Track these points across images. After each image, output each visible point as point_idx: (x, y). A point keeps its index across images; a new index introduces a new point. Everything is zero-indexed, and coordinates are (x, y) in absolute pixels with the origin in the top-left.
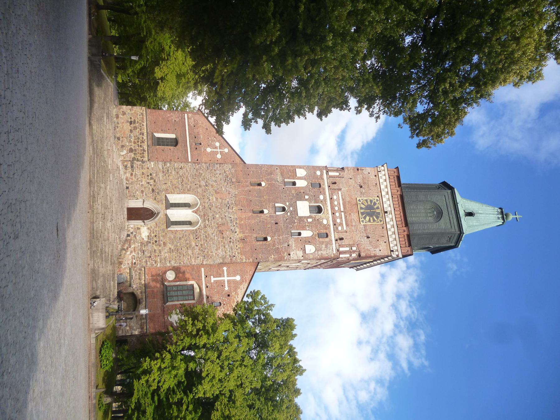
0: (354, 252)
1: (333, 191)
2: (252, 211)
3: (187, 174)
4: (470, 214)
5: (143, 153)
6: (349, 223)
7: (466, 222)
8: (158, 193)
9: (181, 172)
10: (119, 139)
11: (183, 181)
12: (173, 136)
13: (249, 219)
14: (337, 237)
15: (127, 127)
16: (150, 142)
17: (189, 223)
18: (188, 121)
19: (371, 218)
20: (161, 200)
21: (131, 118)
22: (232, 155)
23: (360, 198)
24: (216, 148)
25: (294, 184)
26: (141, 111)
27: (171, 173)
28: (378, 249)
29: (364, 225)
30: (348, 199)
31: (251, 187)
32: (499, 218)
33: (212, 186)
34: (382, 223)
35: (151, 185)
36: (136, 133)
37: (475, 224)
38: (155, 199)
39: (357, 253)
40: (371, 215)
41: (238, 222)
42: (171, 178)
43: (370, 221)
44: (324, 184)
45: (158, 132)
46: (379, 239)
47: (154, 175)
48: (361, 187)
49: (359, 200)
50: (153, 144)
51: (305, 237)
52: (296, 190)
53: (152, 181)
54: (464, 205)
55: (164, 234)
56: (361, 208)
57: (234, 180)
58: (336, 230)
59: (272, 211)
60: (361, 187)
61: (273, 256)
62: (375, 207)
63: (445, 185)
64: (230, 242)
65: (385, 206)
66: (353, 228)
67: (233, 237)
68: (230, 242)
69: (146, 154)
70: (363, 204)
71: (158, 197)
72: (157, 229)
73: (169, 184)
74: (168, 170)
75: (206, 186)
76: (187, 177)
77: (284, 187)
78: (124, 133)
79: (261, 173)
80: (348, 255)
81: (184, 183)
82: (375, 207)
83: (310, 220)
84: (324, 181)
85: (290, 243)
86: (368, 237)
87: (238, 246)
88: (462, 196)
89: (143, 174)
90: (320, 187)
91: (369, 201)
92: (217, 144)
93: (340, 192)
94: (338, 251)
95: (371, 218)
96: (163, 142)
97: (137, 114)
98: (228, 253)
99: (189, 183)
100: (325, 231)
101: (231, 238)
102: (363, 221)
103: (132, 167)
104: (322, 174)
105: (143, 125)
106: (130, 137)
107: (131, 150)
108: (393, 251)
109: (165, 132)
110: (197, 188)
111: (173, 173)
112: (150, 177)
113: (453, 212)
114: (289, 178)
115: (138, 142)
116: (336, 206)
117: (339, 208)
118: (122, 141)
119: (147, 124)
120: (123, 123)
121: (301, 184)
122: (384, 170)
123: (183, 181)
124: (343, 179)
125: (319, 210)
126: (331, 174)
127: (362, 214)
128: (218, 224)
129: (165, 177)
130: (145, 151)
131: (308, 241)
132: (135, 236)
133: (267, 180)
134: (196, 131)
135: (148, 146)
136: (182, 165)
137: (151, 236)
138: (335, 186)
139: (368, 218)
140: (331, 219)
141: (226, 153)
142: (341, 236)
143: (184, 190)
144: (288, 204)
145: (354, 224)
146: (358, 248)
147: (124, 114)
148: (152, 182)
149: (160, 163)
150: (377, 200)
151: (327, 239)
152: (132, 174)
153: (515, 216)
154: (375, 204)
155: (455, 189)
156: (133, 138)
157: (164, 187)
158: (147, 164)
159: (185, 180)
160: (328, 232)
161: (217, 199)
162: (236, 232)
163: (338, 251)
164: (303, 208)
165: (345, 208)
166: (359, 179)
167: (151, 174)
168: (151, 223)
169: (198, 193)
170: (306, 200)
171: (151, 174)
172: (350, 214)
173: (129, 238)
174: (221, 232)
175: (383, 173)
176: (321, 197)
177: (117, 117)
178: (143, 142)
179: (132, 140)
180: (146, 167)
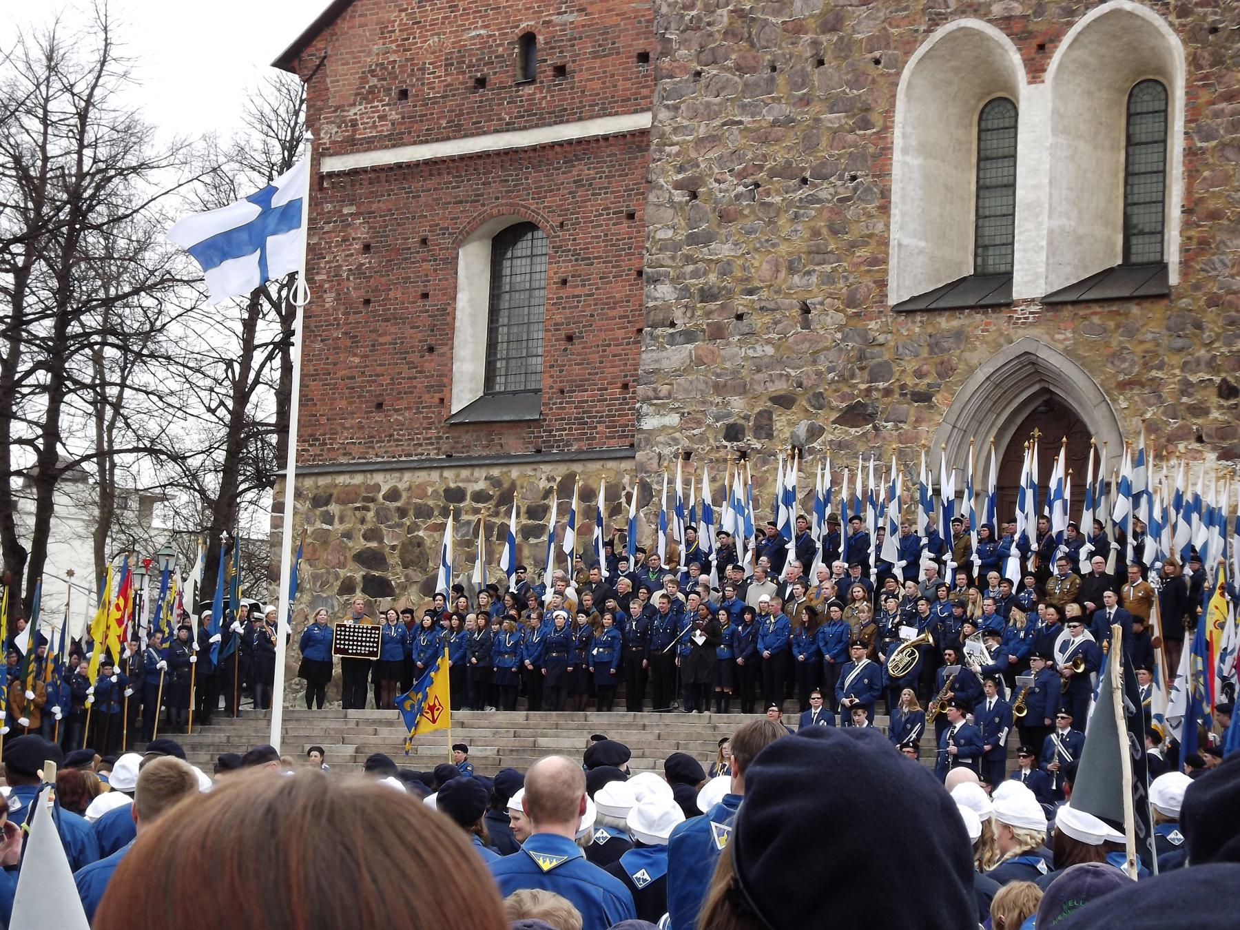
3: (734, 139)
9: (724, 188)
12: (472, 263)
17: (1142, 97)
18: (370, 145)
20: (935, 346)
21: (347, 587)
27: (725, 269)
35: (815, 432)
38: (923, 397)
42: (761, 267)
45: (442, 384)
47: (738, 404)
53: (781, 422)
72: (1170, 379)
73: (807, 284)
74: (707, 295)
81: (806, 164)
97: (324, 537)
99: (804, 116)
105: (393, 495)
110: (845, 47)
111: (724, 250)
119: (387, 469)
123: (785, 171)
129: (758, 321)
134: (436, 80)
135: (539, 455)
136: (666, 177)
149: (649, 358)
157: (829, 321)
159: (779, 155)
167: (733, 433)
169: (882, 40)
171: (733, 433)
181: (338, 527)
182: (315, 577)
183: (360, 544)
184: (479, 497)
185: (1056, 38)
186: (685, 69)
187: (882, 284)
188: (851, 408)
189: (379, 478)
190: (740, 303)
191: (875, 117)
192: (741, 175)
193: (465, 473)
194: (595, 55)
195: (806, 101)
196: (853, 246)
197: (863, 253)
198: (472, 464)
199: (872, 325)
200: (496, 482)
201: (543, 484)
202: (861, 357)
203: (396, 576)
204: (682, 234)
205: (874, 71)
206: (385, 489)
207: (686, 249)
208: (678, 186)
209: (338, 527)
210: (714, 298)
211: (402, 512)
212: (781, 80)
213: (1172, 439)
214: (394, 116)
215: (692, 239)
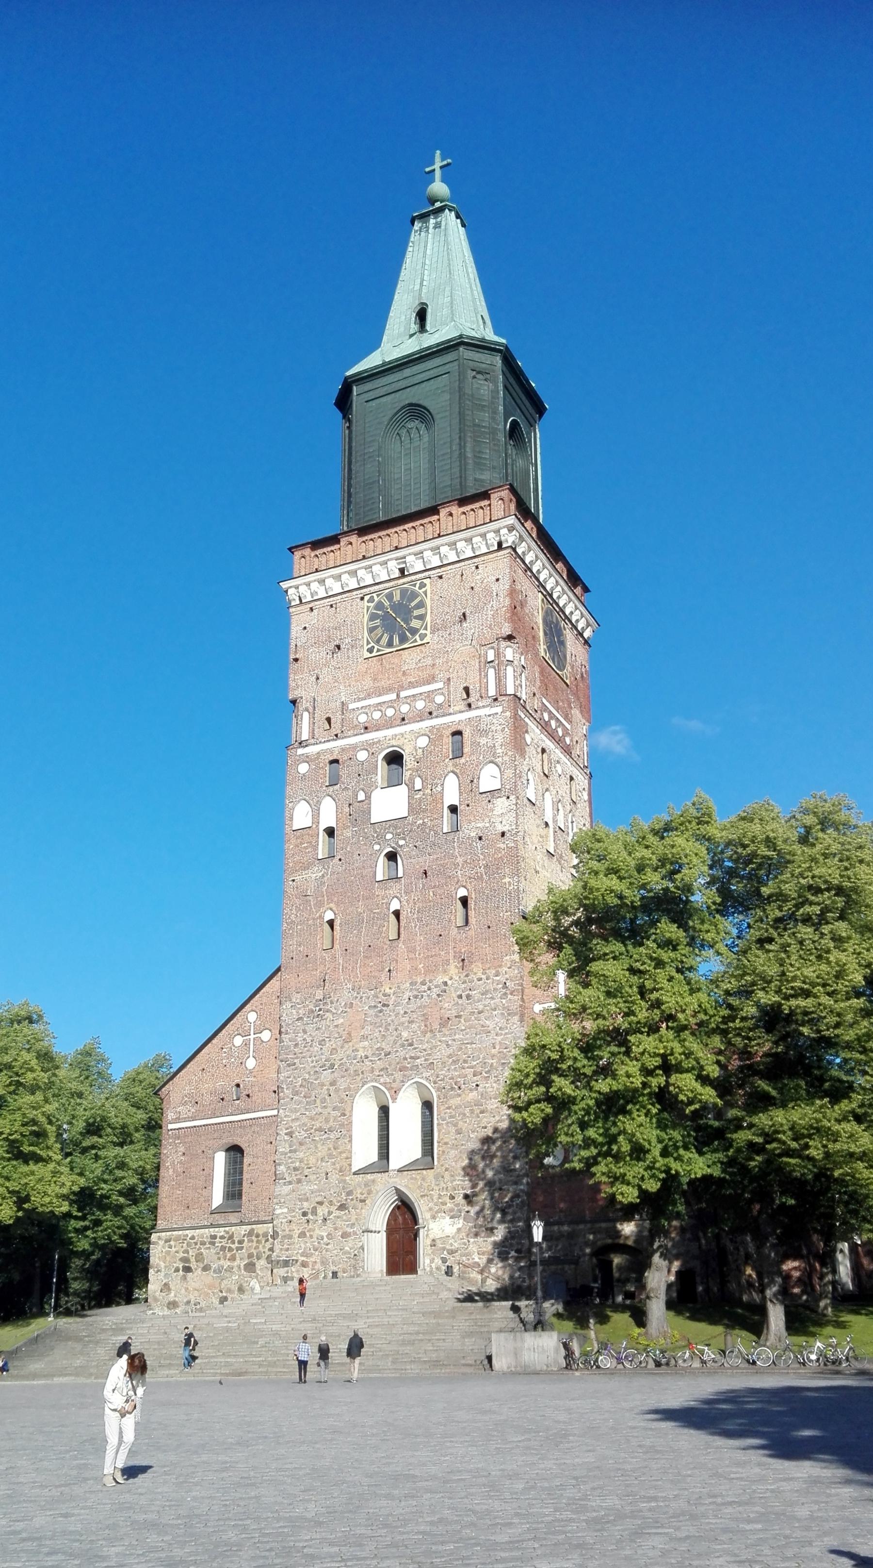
0: (498, 655)
1: (349, 727)
2: (395, 944)
3: (304, 1120)
4: (422, 315)
5: (257, 1236)
6: (425, 675)
7: (439, 333)
8: (349, 1193)
9: (300, 1135)
10: (223, 1300)
11: (320, 1130)
13: (412, 950)
14: (462, 706)
15: (197, 1278)
16: (233, 1218)
19: (416, 613)
20: (366, 1185)
22: (264, 1000)
24: (246, 1044)
25: (330, 832)
26: (161, 1243)
27: (301, 1161)
28: (495, 587)
29: (433, 632)
30: (368, 683)
31: (336, 946)
32: (437, 226)
33: (334, 1051)
34: (427, 581)
35: (330, 1213)
36: (209, 1254)
37: (448, 300)
39: (503, 644)
41: (419, 980)
42: (312, 1160)
44: (331, 751)
45: (209, 1199)
46: (468, 586)
47: (305, 1204)
49: (370, 650)
50: (237, 1210)
51: (461, 793)
52: (345, 827)
54: (397, 341)
55: (447, 1175)
56: (390, 644)
57: (319, 994)
58: (443, 710)
59: (395, 888)
60: (338, 647)
61: (507, 880)
63: (343, 402)
64: (468, 997)
67: (456, 990)
68: (468, 997)
69: (260, 1229)
70: (378, 642)
71: (357, 1193)
72: (435, 1194)
73: (328, 1166)
74: (295, 1169)
75: (332, 1066)
76: (312, 1119)
77: (336, 860)
78: (210, 1287)
79: (301, 923)
80: (510, 670)
81: (326, 1127)
83: (418, 784)
84: (326, 751)
85: (473, 834)
87: (480, 975)
88: (375, 344)
89: (302, 1235)
90: (336, 761)
91: (372, 624)
92: (238, 1041)
93: (351, 706)
94: (496, 700)
95: (416, 613)
96: (234, 1184)
98: (498, 1000)
100: (448, 740)
101: (460, 997)
102: (423, 637)
103: (286, 1263)
104: (307, 759)
105: (193, 1238)
106: (219, 1271)
107: (250, 1267)
108: (500, 544)
109: (210, 1179)
110: (337, 1090)
111: (301, 1155)
112: (310, 1217)
113: (407, 372)
114: (316, 848)
115: (230, 1249)
117: (390, 704)
118: (229, 1291)
120: (186, 1289)
121: (328, 818)
122: (297, 587)
123: (320, 1130)
124: (318, 699)
125: (395, 759)
128: (424, 1033)
130: (253, 1230)
131: (469, 784)
132: (452, 1252)
133: (320, 904)
134: (207, 1099)
135: (242, 1223)
137: (451, 1210)
139: (415, 623)
140: (415, 726)
141: (259, 1017)
143: (342, 1125)
144: (377, 847)
145: (429, 661)
147: (166, 1287)
148: (322, 1211)
150: (371, 600)
151: (466, 734)
152: (304, 1265)
153: (438, 174)
154: (380, 606)
155: (348, 374)
156: (222, 1262)
157: (334, 1178)
158: (281, 1223)
161: (364, 1038)
162: (445, 984)
163: (496, 700)
164: (389, 803)
165: (389, 690)
168: (422, 1209)
169: (349, 1089)
170: (368, 797)
171: (305, 1214)
172: (404, 673)
173: (456, 1269)
174: (445, 1022)
176: (362, 756)
177: (173, 1305)
178: (231, 1237)
179: (226, 1264)
180: (286, 1226)
181: (174, 1249)
182: (166, 1267)
183: (181, 1255)
184: (222, 1237)
185: (400, 1089)
186: (288, 1097)
187: (350, 1165)
188: (341, 1205)
189: (187, 1232)
190: (306, 1172)
191: (346, 1113)
192: (306, 1131)
193: (217, 1229)
194: (259, 1091)
195: (325, 1107)
196: (341, 1153)
197: (344, 1155)
198: (219, 1226)
199: (347, 1178)
200: (227, 1232)
201: (243, 1233)
202: (344, 1188)
203: (193, 1265)
204: (288, 1150)
205: (346, 1099)
206: (190, 1236)
207: (289, 1155)
208: (286, 1134)
209: (174, 1249)
210: (298, 1170)
211: (196, 1244)
212: (318, 1101)
213: (437, 1212)
214: (193, 1110)
215: (291, 1151)
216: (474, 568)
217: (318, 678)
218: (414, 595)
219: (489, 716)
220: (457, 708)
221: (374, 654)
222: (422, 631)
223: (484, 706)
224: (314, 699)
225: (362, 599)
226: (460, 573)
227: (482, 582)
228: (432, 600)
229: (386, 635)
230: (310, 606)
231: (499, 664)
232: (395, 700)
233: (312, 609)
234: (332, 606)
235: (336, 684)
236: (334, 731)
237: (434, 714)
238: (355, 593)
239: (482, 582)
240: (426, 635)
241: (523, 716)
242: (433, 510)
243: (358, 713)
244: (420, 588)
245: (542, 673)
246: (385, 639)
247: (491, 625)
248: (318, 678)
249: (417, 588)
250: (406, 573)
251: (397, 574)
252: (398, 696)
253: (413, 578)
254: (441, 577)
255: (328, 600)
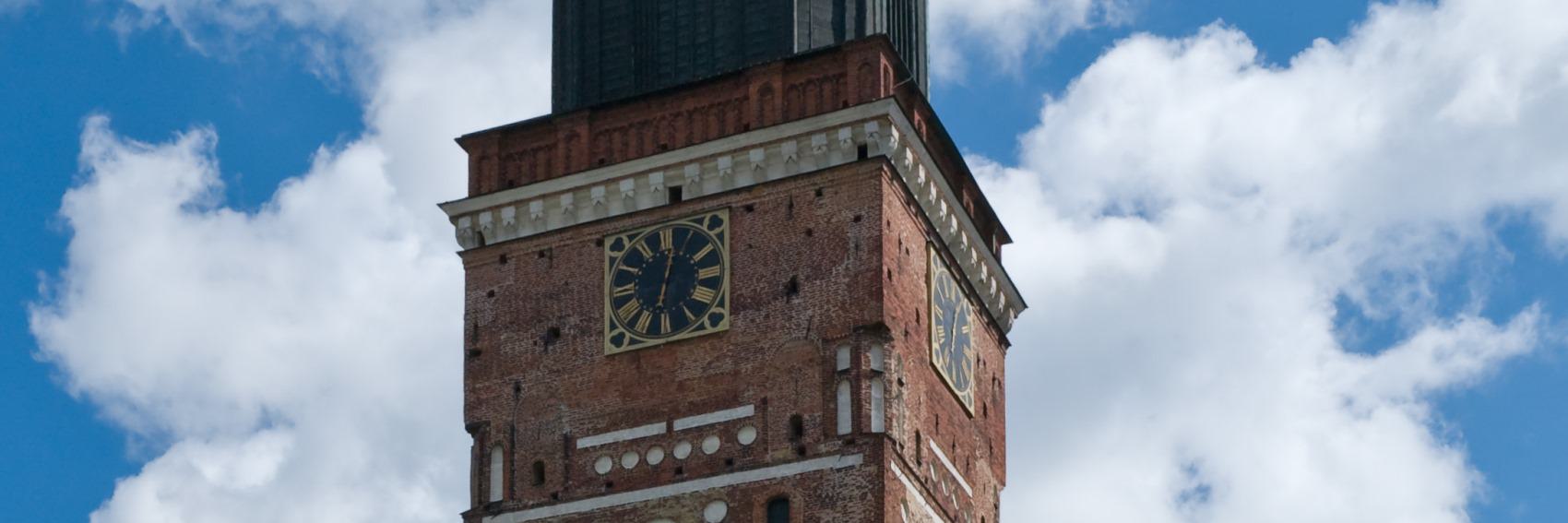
0: (856, 359)
14: (786, 450)
19: (704, 274)
23: (608, 335)
29: (734, 311)
30: (613, 401)
34: (725, 216)
40: (684, 275)
43: (713, 283)
48: (555, 334)
49: (617, 341)
56: (654, 330)
58: (751, 457)
60: (555, 334)
62: (647, 254)
65: (645, 203)
66: (746, 367)
70: (631, 324)
82: (647, 254)
86: (793, 288)
93: (582, 443)
94: (849, 443)
95: (704, 274)
102: (716, 319)
108: (862, 150)
116: (643, 461)
122: (477, 213)
124: (521, 428)
126: (497, 494)
127: (679, 323)
138: (555, 466)
139: (701, 294)
142: (783, 427)
145: (728, 365)
146: (842, 341)
150: (618, 246)
151: (797, 501)
154: (633, 258)
160: (761, 499)
165: (650, 417)
166: (520, 344)
172: (681, 387)
175: (485, 219)
216: (813, 193)
217: (518, 389)
218: (701, 240)
219: (839, 470)
220: (779, 455)
221: (624, 348)
222: (714, 310)
223: (829, 454)
224: (513, 429)
225: (600, 243)
226: (787, 203)
227: (829, 222)
228: (732, 250)
229: (646, 313)
230: (500, 252)
231: (856, 376)
232: (663, 436)
233: (503, 260)
234: (541, 254)
235: (552, 401)
236: (551, 488)
237: (738, 464)
238: (586, 230)
239: (829, 222)
240: (721, 317)
241: (898, 472)
242: (738, 76)
243: (594, 455)
244: (711, 227)
245: (931, 393)
246: (645, 320)
247: (843, 303)
248: (518, 389)
249: (705, 228)
250: (685, 197)
251: (663, 199)
252: (670, 427)
253: (698, 207)
254: (750, 209)
255: (535, 242)
